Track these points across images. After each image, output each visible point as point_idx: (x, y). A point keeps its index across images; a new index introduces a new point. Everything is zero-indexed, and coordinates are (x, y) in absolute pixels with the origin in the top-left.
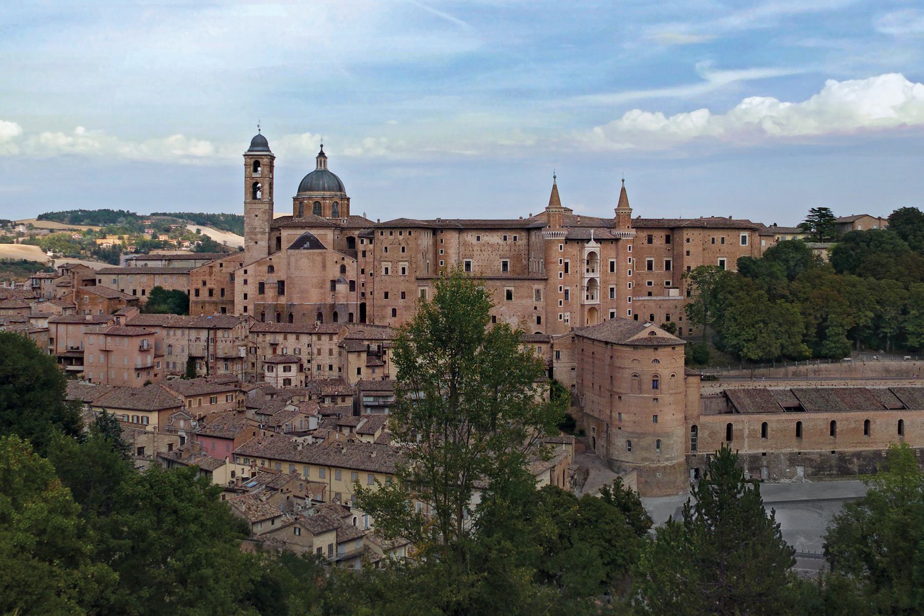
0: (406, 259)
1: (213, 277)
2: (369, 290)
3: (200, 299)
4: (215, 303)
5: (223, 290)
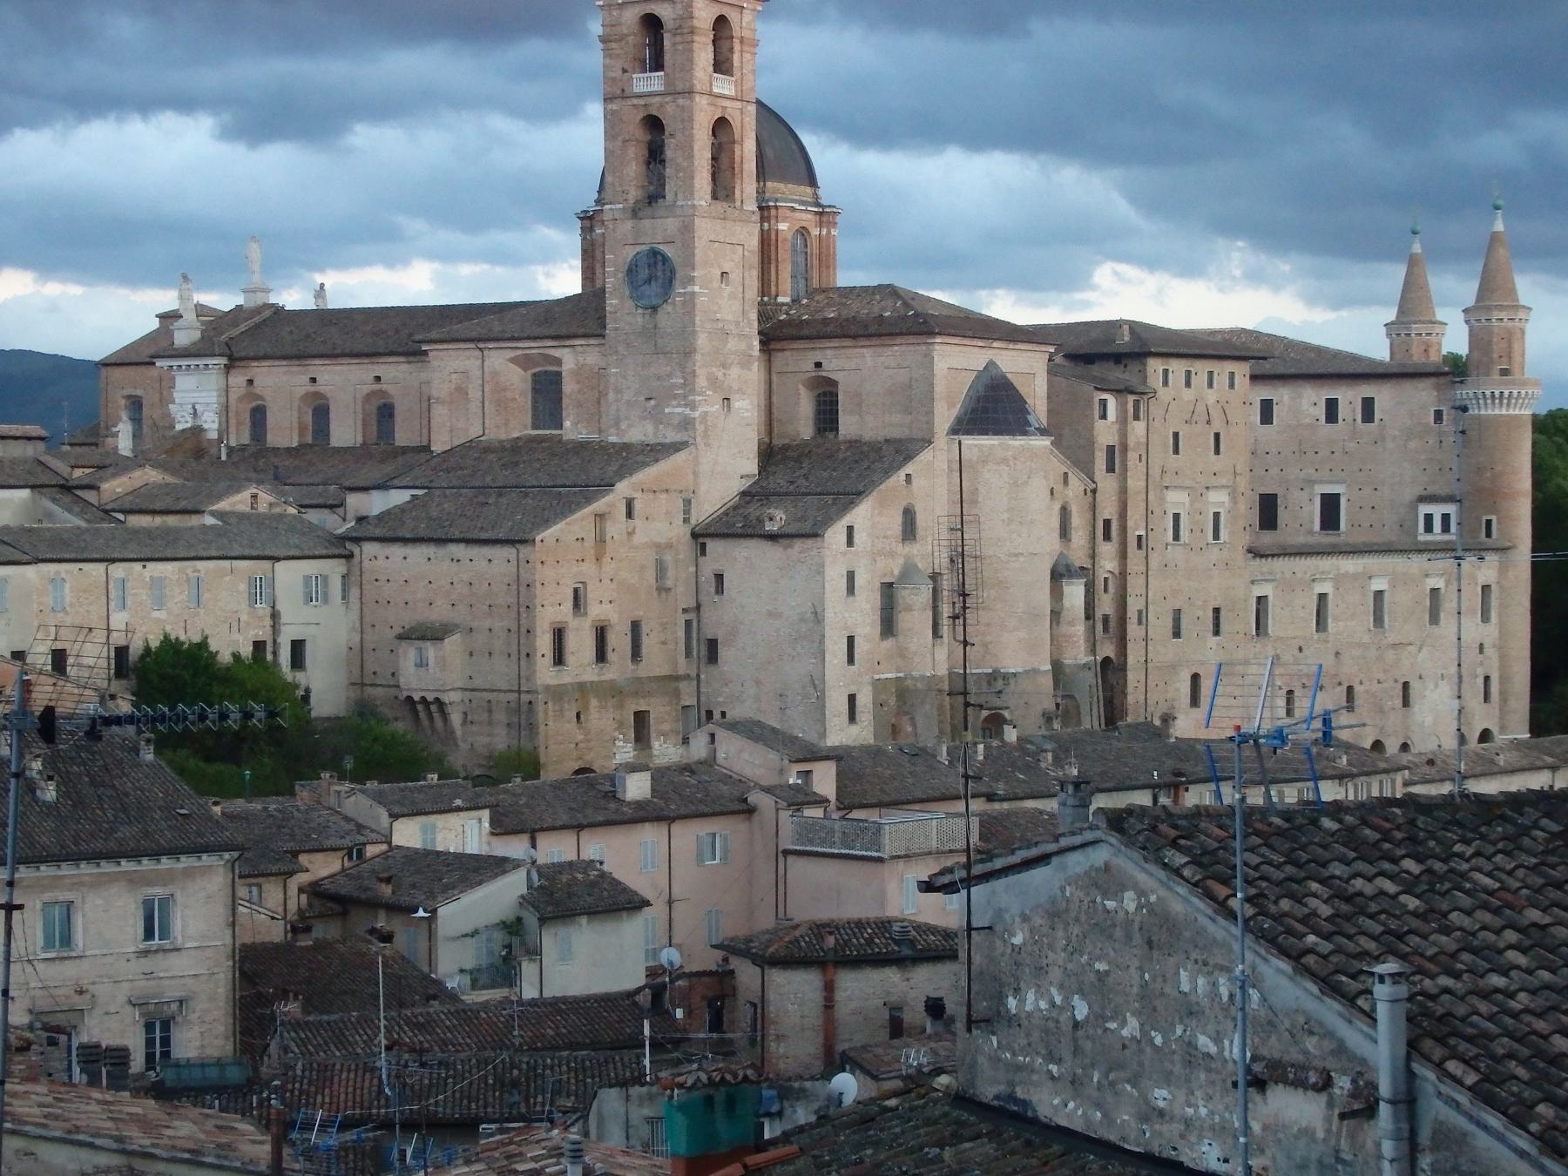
0: (1224, 482)
1: (609, 568)
2: (1134, 605)
3: (567, 676)
4: (613, 692)
5: (636, 627)
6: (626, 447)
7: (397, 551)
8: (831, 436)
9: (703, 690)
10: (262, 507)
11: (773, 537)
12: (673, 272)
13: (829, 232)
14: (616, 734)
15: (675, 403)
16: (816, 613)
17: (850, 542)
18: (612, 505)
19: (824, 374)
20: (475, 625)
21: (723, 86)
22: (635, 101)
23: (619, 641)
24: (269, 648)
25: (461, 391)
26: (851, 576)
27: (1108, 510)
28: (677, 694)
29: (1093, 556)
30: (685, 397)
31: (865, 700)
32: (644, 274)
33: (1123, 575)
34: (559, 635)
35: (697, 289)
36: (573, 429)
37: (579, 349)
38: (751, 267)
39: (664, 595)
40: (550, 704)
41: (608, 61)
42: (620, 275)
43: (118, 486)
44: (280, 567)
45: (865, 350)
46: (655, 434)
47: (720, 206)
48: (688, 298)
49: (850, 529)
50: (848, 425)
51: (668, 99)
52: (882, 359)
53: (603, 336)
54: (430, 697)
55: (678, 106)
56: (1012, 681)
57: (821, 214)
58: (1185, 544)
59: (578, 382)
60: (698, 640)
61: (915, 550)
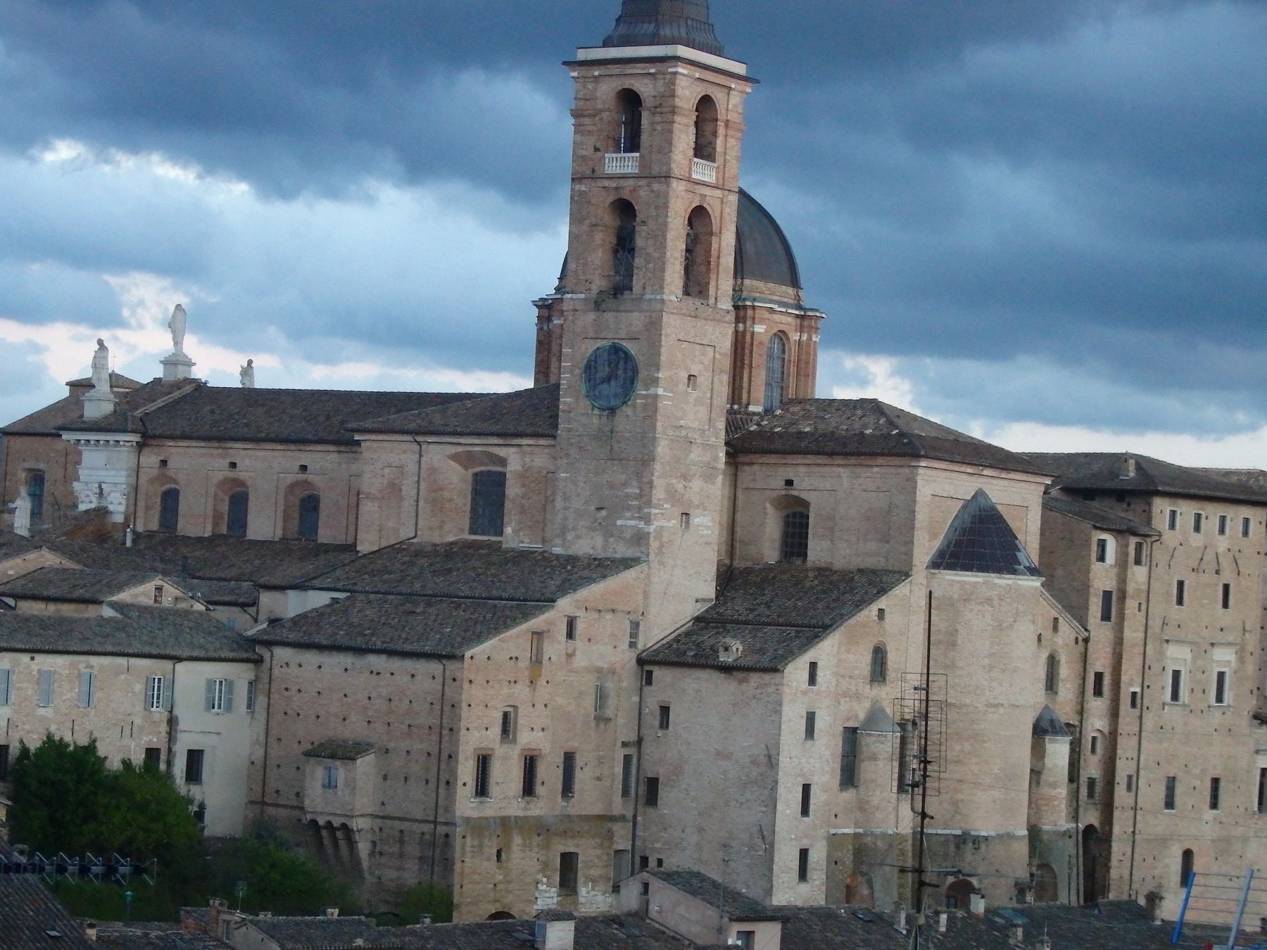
0: (1231, 639)
1: (543, 691)
2: (1123, 769)
3: (492, 808)
4: (541, 830)
5: (569, 758)
6: (572, 560)
7: (311, 658)
8: (798, 562)
9: (639, 833)
10: (167, 601)
11: (727, 669)
12: (635, 371)
13: (810, 338)
14: (540, 876)
15: (628, 514)
16: (770, 757)
17: (812, 680)
18: (552, 623)
19: (795, 493)
20: (391, 745)
21: (704, 172)
22: (606, 183)
23: (549, 774)
24: (163, 757)
25: (394, 489)
26: (811, 718)
27: (1100, 661)
28: (610, 835)
29: (1081, 712)
30: (640, 509)
31: (818, 856)
32: (603, 371)
33: (1112, 736)
34: (484, 763)
35: (660, 391)
36: (514, 536)
37: (528, 449)
38: (721, 371)
39: (602, 726)
40: (468, 839)
41: (579, 138)
42: (577, 371)
43: (11, 568)
44: (181, 667)
45: (841, 470)
46: (605, 548)
47: (691, 302)
48: (650, 401)
49: (813, 666)
50: (818, 551)
51: (642, 182)
52: (860, 481)
53: (554, 437)
54: (337, 822)
55: (652, 191)
56: (983, 847)
57: (802, 317)
58: (1184, 705)
59: (524, 485)
60: (638, 780)
61: (886, 695)
